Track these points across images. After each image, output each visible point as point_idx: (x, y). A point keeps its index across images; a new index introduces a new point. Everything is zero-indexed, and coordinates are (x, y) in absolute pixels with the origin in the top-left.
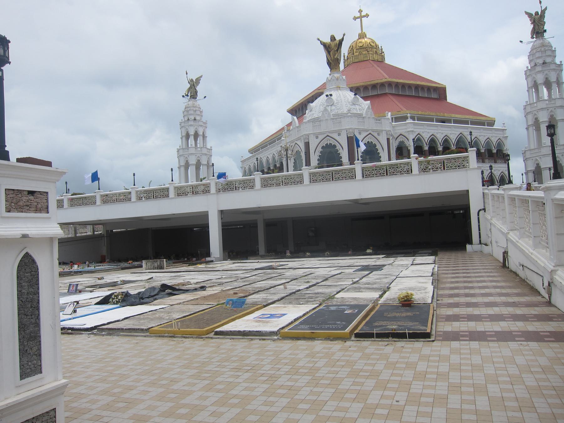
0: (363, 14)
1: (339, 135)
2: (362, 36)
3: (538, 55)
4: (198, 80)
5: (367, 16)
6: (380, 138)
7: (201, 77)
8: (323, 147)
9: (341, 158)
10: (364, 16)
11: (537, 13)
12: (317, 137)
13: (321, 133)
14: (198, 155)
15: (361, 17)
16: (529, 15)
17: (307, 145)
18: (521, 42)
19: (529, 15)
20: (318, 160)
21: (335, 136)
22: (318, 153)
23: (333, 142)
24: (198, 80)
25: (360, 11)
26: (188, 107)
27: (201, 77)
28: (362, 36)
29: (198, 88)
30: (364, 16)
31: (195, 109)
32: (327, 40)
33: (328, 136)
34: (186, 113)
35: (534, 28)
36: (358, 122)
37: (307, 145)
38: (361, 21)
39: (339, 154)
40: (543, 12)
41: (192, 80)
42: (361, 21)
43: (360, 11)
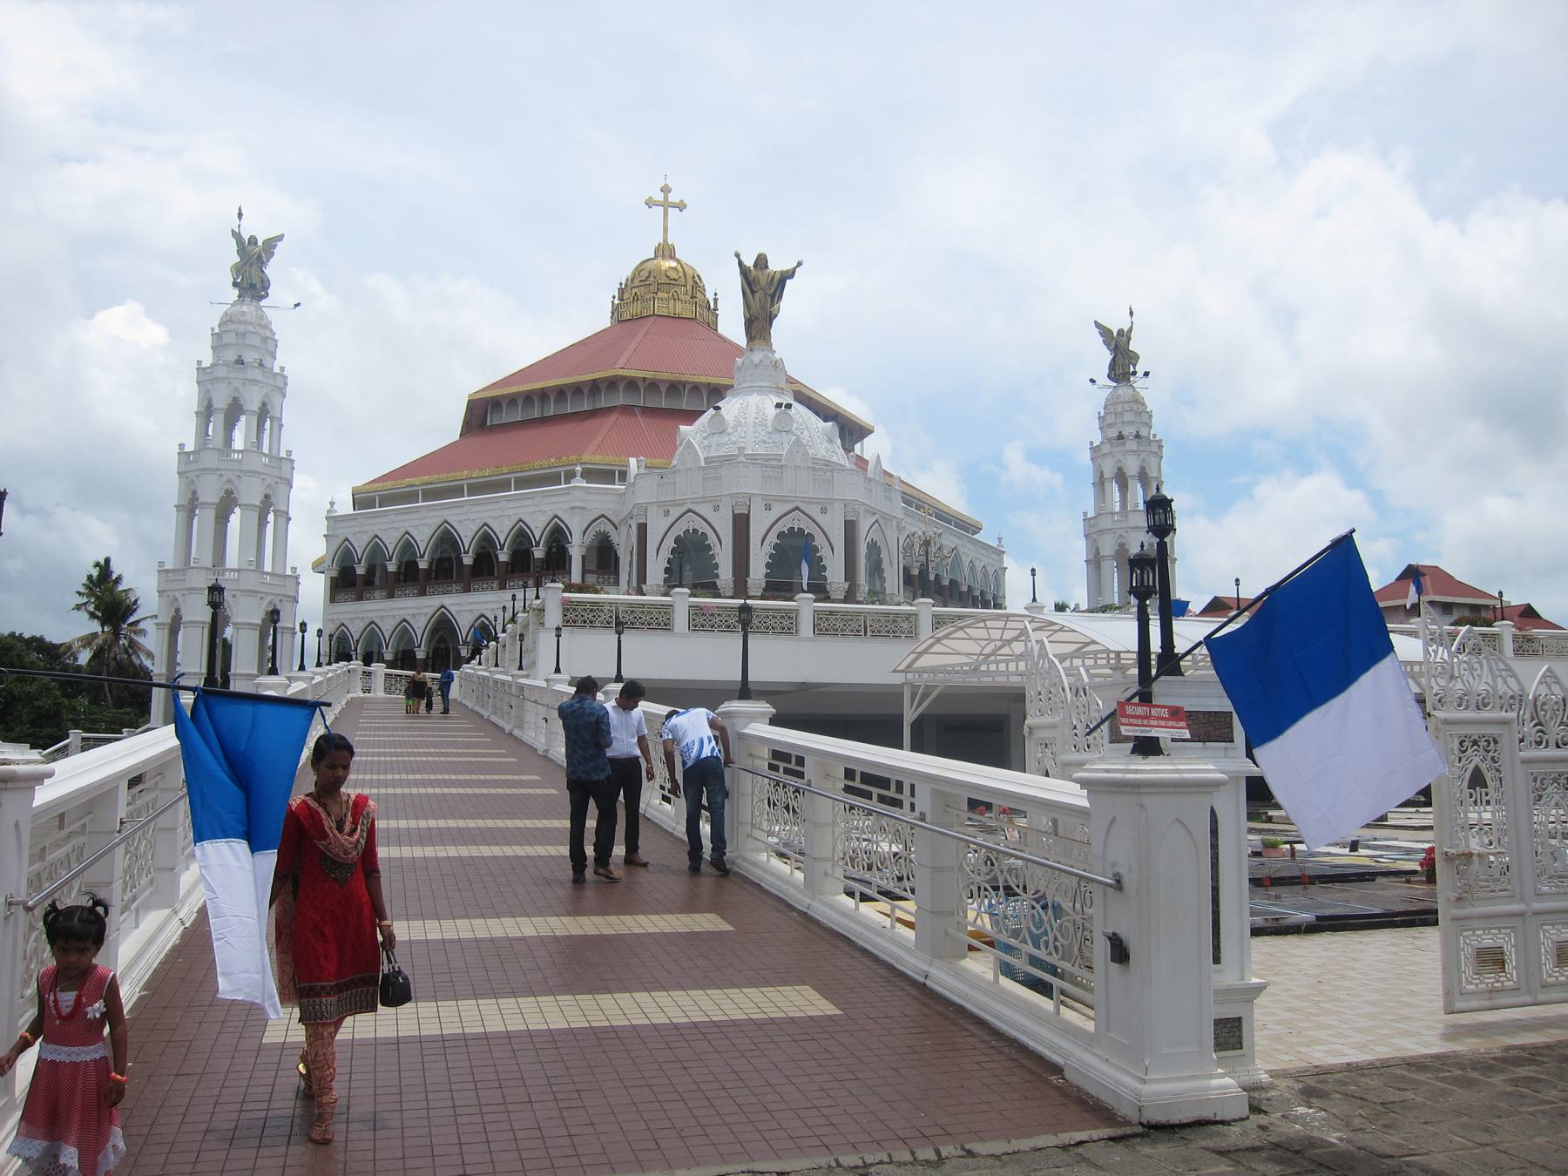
0: (673, 198)
1: (824, 510)
2: (665, 250)
3: (1128, 417)
4: (271, 244)
5: (681, 206)
6: (888, 533)
7: (280, 238)
8: (781, 535)
9: (824, 568)
10: (674, 206)
11: (1121, 332)
12: (768, 507)
13: (782, 499)
14: (269, 480)
16: (1105, 332)
17: (741, 524)
18: (1092, 381)
19: (1105, 332)
20: (768, 565)
21: (814, 511)
24: (271, 244)
25: (666, 190)
26: (239, 322)
27: (280, 238)
28: (665, 250)
29: (271, 271)
30: (674, 206)
31: (242, 328)
32: (749, 262)
33: (797, 508)
34: (230, 338)
35: (1114, 360)
36: (764, 478)
37: (741, 524)
38: (666, 215)
39: (821, 559)
41: (253, 241)
42: (666, 215)
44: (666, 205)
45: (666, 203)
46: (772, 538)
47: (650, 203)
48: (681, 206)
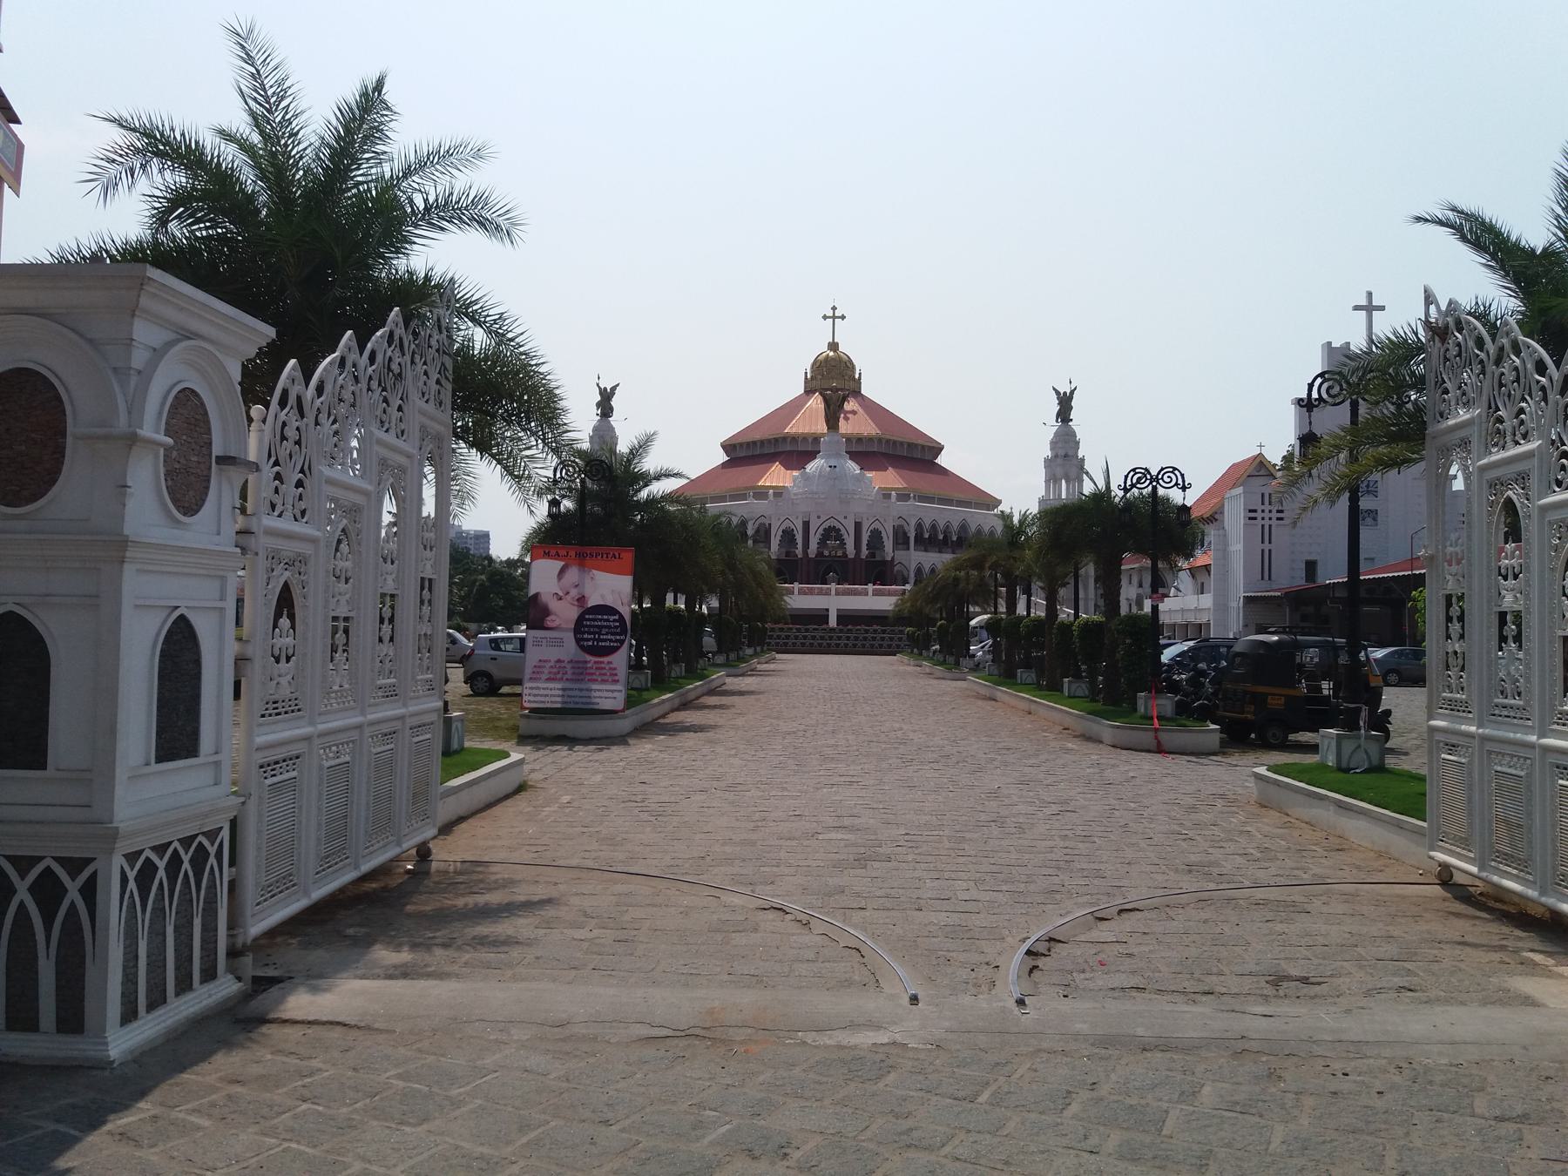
4: (614, 389)
5: (843, 317)
15: (834, 317)
17: (806, 525)
22: (818, 536)
23: (838, 525)
24: (614, 389)
25: (834, 308)
28: (833, 346)
29: (615, 402)
37: (806, 525)
40: (1072, 392)
43: (834, 308)
44: (834, 317)
45: (834, 317)
46: (821, 531)
47: (825, 317)
48: (843, 317)
